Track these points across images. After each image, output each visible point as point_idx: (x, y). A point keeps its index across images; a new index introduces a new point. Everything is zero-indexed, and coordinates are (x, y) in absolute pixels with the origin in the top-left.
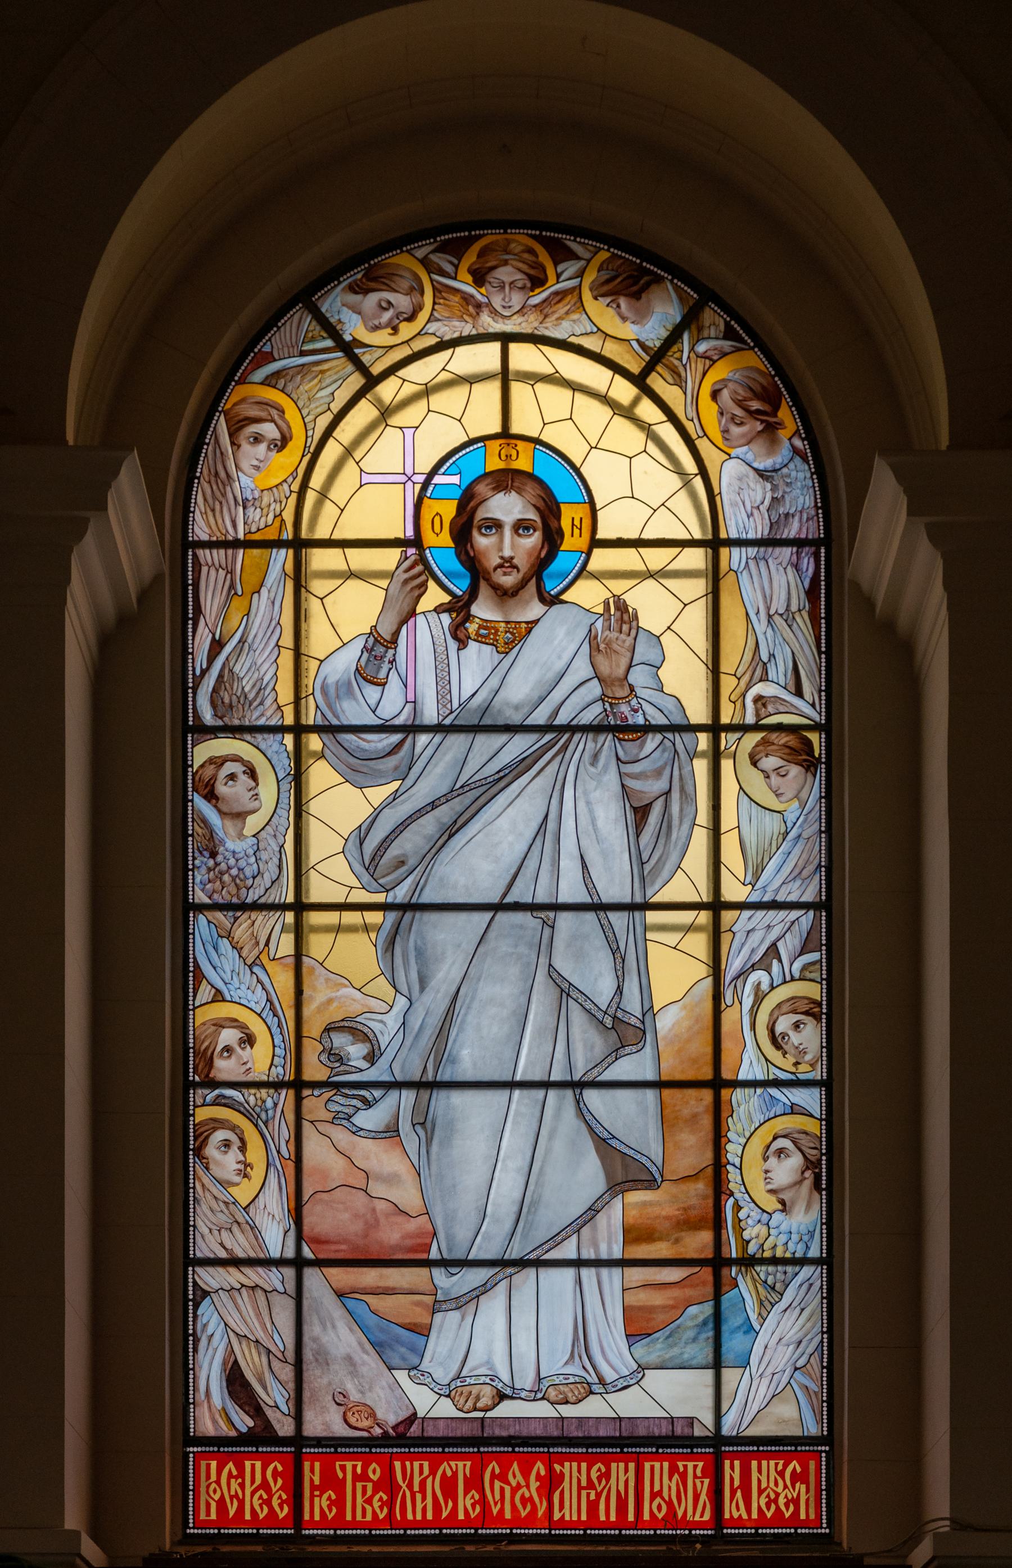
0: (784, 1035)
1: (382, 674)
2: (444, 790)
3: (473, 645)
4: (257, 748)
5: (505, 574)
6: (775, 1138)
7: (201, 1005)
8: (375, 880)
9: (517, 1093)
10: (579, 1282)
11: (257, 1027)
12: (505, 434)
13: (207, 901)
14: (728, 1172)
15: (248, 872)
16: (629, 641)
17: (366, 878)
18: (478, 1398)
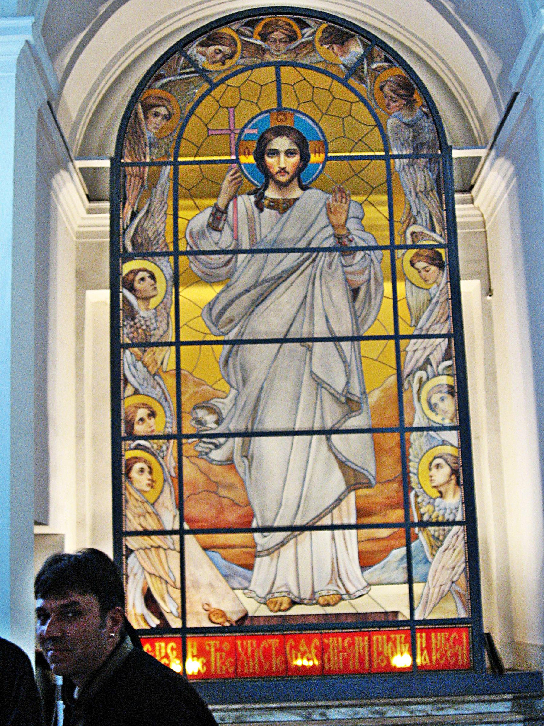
0: (436, 405)
1: (220, 226)
2: (252, 283)
3: (266, 210)
4: (155, 264)
5: (282, 176)
6: (435, 458)
7: (128, 397)
8: (219, 329)
9: (296, 438)
10: (333, 539)
11: (157, 408)
12: (280, 109)
13: (130, 342)
14: (410, 477)
15: (152, 327)
16: (346, 207)
17: (214, 328)
18: (281, 604)
